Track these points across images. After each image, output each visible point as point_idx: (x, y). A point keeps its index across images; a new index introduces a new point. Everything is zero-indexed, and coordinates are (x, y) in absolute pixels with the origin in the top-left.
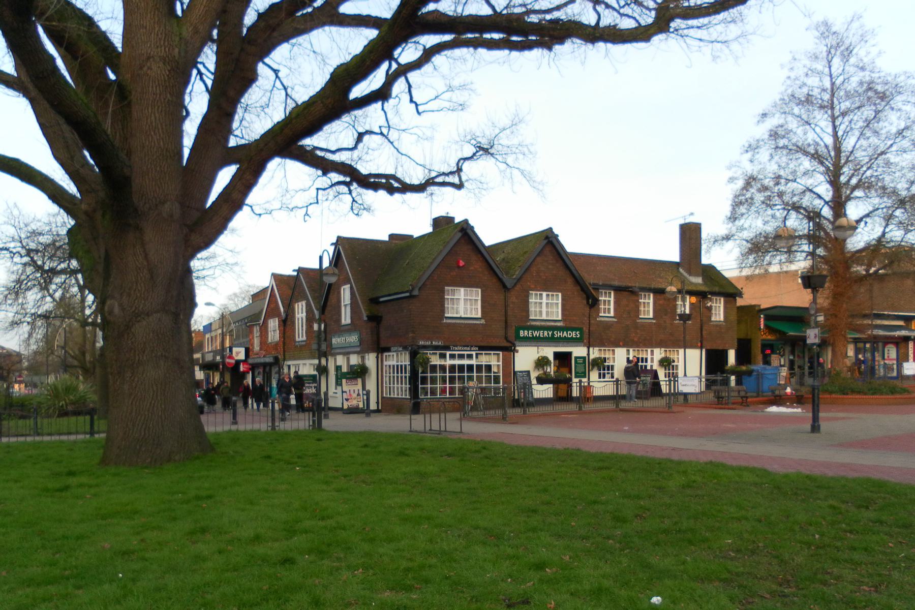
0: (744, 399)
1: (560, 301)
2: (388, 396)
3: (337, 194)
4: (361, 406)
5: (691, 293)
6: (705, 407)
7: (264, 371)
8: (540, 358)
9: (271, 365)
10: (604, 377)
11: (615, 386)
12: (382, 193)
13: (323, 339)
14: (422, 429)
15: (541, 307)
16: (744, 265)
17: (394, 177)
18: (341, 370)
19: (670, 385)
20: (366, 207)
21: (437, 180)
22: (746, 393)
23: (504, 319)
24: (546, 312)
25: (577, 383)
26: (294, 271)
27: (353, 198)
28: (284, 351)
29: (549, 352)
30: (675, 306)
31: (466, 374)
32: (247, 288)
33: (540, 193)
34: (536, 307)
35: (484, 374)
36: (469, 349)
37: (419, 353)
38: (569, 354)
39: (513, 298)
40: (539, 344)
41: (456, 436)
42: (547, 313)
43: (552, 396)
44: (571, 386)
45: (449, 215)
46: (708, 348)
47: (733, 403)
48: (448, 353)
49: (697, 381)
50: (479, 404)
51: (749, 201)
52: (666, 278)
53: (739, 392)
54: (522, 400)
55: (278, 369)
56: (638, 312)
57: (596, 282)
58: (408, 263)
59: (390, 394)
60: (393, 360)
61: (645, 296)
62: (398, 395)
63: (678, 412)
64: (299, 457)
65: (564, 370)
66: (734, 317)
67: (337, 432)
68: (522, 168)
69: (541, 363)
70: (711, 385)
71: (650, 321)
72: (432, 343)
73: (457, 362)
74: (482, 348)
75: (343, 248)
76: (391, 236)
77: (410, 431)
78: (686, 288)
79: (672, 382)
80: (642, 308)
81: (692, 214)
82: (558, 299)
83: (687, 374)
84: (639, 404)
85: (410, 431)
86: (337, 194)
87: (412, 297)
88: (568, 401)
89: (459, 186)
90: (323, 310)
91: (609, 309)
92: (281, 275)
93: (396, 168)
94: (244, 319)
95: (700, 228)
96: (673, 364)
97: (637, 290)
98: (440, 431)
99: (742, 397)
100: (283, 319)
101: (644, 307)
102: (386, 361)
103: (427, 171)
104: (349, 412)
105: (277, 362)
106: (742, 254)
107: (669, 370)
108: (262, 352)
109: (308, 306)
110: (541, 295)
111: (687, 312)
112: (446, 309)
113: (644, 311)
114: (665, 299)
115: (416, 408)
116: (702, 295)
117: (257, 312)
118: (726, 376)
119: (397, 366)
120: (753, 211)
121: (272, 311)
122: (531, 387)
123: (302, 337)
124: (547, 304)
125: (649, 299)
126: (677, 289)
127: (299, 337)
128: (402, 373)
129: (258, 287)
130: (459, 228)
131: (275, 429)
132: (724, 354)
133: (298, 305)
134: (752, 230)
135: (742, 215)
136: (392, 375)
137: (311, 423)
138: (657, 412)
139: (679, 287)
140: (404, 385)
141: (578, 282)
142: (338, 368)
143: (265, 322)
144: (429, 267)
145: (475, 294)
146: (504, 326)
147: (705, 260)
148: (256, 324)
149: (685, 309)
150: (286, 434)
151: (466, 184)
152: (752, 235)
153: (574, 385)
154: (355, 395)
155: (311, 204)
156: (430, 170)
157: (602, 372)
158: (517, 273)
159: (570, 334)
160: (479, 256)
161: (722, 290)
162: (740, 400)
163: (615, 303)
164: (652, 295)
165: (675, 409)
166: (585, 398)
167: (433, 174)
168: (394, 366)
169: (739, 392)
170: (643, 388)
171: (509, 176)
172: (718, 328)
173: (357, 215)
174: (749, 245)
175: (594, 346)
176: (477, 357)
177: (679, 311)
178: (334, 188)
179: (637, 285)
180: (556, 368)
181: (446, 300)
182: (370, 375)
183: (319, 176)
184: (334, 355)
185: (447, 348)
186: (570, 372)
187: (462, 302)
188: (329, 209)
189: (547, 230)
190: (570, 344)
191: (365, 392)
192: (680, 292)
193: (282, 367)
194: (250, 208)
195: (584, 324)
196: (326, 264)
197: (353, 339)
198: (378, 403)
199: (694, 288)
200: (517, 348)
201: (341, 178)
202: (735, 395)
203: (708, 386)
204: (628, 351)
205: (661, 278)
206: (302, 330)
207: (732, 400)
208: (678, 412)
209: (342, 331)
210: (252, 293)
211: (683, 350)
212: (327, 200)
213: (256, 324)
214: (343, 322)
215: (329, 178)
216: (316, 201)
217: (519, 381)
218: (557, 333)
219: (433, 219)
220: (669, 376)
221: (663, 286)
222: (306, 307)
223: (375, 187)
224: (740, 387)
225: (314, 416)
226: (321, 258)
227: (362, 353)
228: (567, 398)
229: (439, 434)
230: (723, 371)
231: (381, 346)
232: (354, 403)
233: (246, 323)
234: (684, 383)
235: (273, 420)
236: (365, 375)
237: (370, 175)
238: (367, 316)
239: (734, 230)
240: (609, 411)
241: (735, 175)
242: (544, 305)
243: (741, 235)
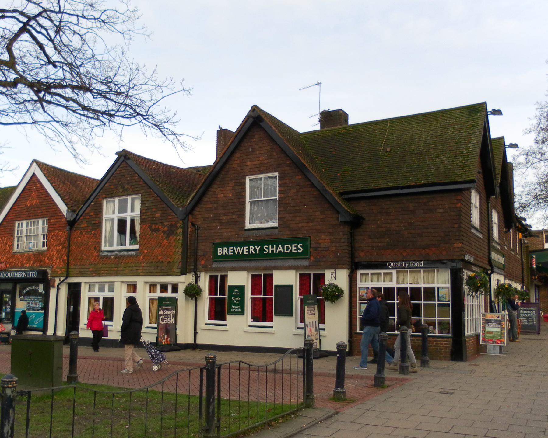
218: (268, 248)
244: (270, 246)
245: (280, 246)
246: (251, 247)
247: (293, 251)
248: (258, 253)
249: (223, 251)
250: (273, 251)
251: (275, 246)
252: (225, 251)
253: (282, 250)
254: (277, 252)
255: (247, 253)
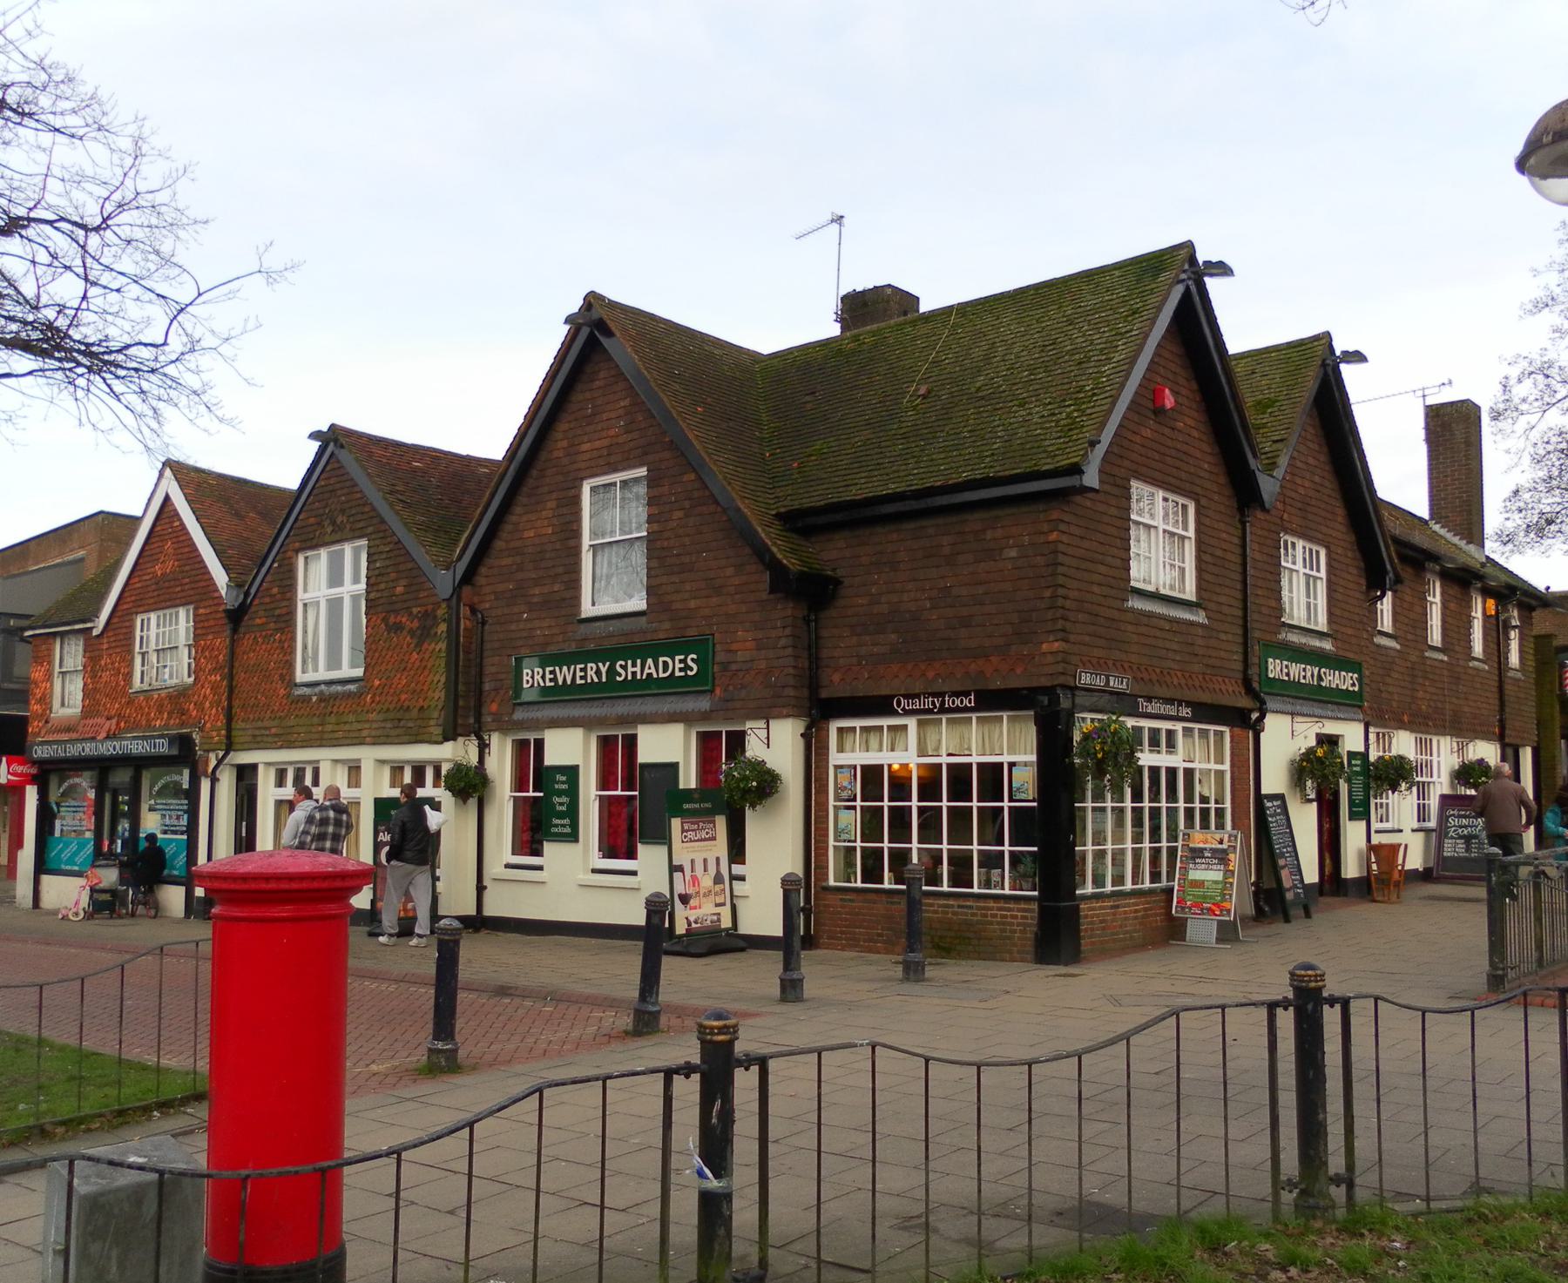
218: (624, 667)
244: (630, 662)
245: (650, 661)
246: (589, 665)
247: (678, 674)
248: (604, 680)
251: (639, 661)
253: (653, 671)
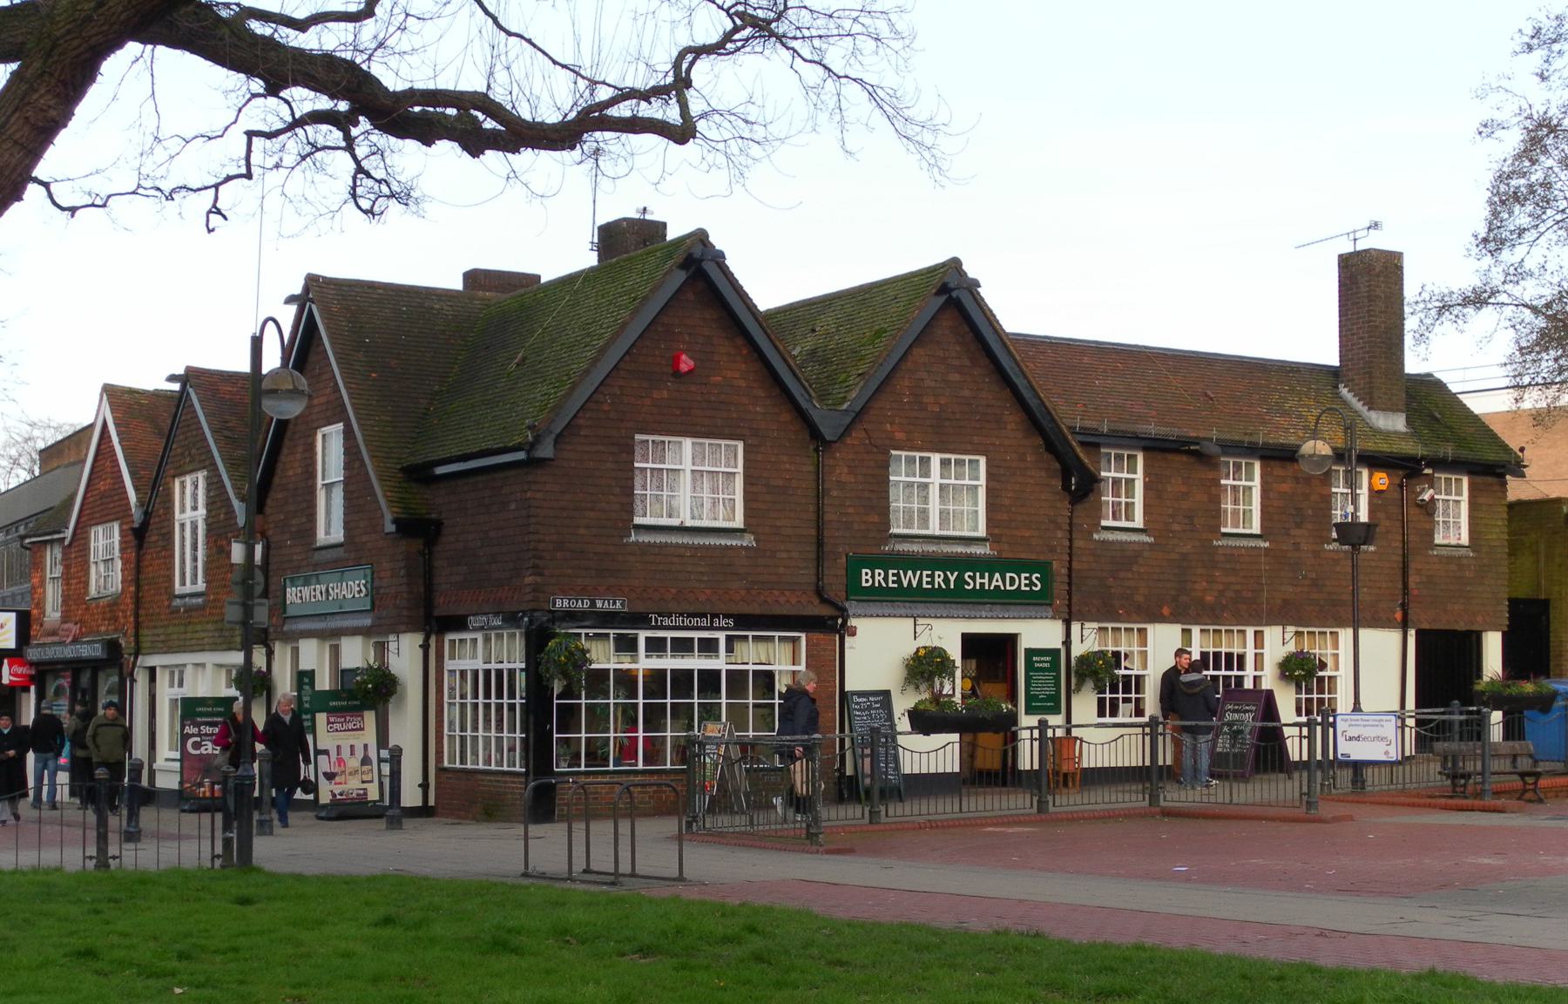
0: (1530, 780)
1: (982, 481)
2: (458, 765)
3: (308, 149)
4: (373, 795)
5: (1374, 461)
6: (1413, 805)
7: (74, 686)
8: (922, 652)
9: (95, 666)
10: (1114, 713)
11: (1148, 739)
12: (447, 150)
13: (259, 589)
14: (563, 868)
15: (925, 499)
16: (1526, 380)
17: (484, 102)
18: (312, 684)
19: (1311, 738)
20: (395, 187)
21: (614, 112)
22: (1536, 762)
23: (813, 532)
24: (941, 512)
25: (1031, 729)
26: (172, 378)
27: (357, 162)
28: (137, 626)
29: (947, 634)
30: (1327, 501)
31: (696, 701)
32: (25, 430)
33: (926, 154)
34: (909, 499)
35: (751, 701)
36: (705, 622)
37: (554, 635)
38: (1008, 642)
39: (840, 469)
40: (920, 609)
41: (665, 891)
42: (944, 515)
43: (957, 770)
44: (1014, 738)
45: (648, 217)
46: (1426, 626)
47: (1498, 794)
48: (642, 635)
49: (1389, 728)
50: (737, 791)
51: (1540, 191)
52: (1300, 416)
53: (1514, 757)
54: (868, 781)
55: (115, 679)
56: (1216, 515)
57: (1088, 424)
58: (524, 359)
59: (463, 761)
60: (474, 657)
61: (1238, 467)
62: (488, 761)
63: (1335, 819)
64: (182, 956)
65: (994, 691)
66: (1498, 533)
67: (299, 877)
68: (870, 78)
69: (926, 666)
70: (1432, 739)
71: (1252, 543)
72: (593, 604)
73: (669, 663)
74: (745, 621)
75: (325, 311)
76: (472, 277)
77: (525, 875)
78: (1361, 445)
79: (1319, 728)
80: (1228, 506)
81: (1375, 226)
82: (977, 474)
83: (1363, 707)
84: (1218, 793)
85: (525, 875)
86: (308, 149)
87: (533, 463)
88: (1004, 784)
89: (682, 133)
90: (260, 498)
91: (1130, 506)
92: (132, 391)
93: (491, 74)
94: (16, 523)
95: (1400, 268)
96: (1321, 674)
97: (1214, 449)
98: (616, 874)
99: (1523, 775)
100: (136, 525)
101: (1236, 502)
102: (452, 657)
103: (582, 84)
104: (333, 814)
105: (115, 659)
106: (1521, 349)
107: (1309, 691)
108: (66, 626)
109: (214, 485)
110: (925, 462)
111: (1363, 517)
112: (638, 502)
113: (1235, 513)
114: (1296, 479)
115: (543, 806)
116: (1406, 468)
117: (56, 502)
118: (1478, 712)
119: (487, 673)
120: (1550, 223)
121: (104, 504)
122: (894, 739)
123: (194, 581)
124: (942, 488)
125: (1250, 478)
126: (1334, 449)
127: (183, 583)
128: (500, 695)
129: (71, 425)
130: (679, 257)
131: (107, 866)
132: (1470, 645)
133: (183, 487)
134: (1548, 276)
135: (1521, 231)
136: (469, 700)
137: (219, 850)
138: (1273, 819)
139: (1340, 444)
140: (505, 734)
141: (1038, 423)
142: (304, 678)
143: (81, 538)
144: (587, 372)
145: (728, 459)
146: (814, 556)
147: (1414, 363)
148: (52, 542)
149: (1356, 509)
150: (142, 881)
151: (701, 126)
152: (1549, 293)
153: (1025, 734)
154: (354, 763)
155: (229, 178)
156: (593, 83)
157: (1108, 696)
158: (854, 394)
159: (1012, 579)
160: (740, 341)
161: (1464, 454)
162: (1516, 782)
163: (1147, 487)
164: (1257, 466)
165: (1325, 810)
166: (1057, 773)
167: (604, 94)
168: (476, 673)
169: (1514, 757)
170: (1233, 746)
171: (832, 103)
172: (1454, 567)
173: (369, 212)
174: (1541, 322)
175: (1084, 618)
176: (730, 649)
177: (1337, 516)
178: (299, 131)
179: (1214, 434)
180: (969, 684)
181: (637, 472)
182: (402, 698)
183: (254, 96)
184: (292, 638)
185: (641, 620)
186: (1012, 696)
187: (685, 480)
188: (283, 194)
189: (943, 265)
190: (1014, 611)
191: (385, 754)
192: (1340, 456)
193: (132, 674)
194: (42, 189)
195: (1052, 550)
196: (272, 359)
197: (352, 588)
198: (425, 786)
199: (1384, 447)
200: (853, 622)
201: (324, 103)
202: (1502, 769)
203: (1422, 742)
204: (1187, 633)
205: (1285, 414)
206: (195, 559)
207: (1494, 782)
208: (1335, 819)
209: (316, 566)
210: (41, 445)
211: (1350, 631)
212: (277, 166)
213: (52, 542)
214: (322, 537)
215: (287, 102)
216: (243, 170)
217: (857, 722)
218: (973, 578)
219: (600, 228)
220: (1308, 712)
221: (1292, 440)
222: (208, 490)
223: (426, 131)
224: (1516, 745)
225: (227, 827)
226: (257, 343)
227: (379, 634)
228: (1005, 776)
229: (613, 884)
230: (1468, 697)
231: (436, 613)
232: (352, 785)
233: (23, 538)
234: (1353, 732)
235: (102, 840)
236: (386, 701)
237: (412, 95)
238: (395, 521)
239: (1497, 278)
240: (1129, 815)
241: (1499, 117)
242: (934, 492)
243: (1515, 290)
244: (978, 574)
246: (937, 573)
248: (952, 587)
249: (873, 577)
250: (982, 585)
251: (987, 574)
252: (879, 578)
253: (1000, 583)
254: (992, 588)
255: (930, 586)
